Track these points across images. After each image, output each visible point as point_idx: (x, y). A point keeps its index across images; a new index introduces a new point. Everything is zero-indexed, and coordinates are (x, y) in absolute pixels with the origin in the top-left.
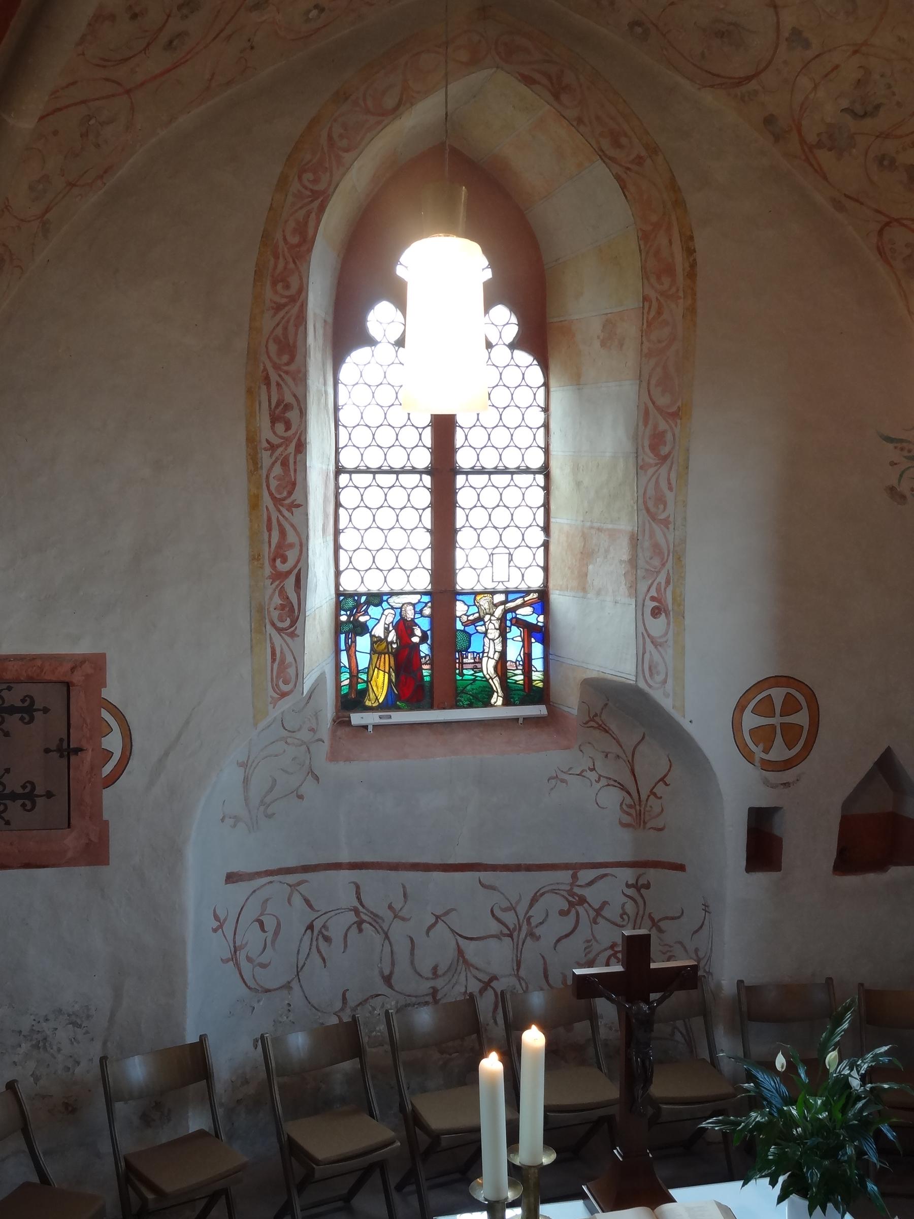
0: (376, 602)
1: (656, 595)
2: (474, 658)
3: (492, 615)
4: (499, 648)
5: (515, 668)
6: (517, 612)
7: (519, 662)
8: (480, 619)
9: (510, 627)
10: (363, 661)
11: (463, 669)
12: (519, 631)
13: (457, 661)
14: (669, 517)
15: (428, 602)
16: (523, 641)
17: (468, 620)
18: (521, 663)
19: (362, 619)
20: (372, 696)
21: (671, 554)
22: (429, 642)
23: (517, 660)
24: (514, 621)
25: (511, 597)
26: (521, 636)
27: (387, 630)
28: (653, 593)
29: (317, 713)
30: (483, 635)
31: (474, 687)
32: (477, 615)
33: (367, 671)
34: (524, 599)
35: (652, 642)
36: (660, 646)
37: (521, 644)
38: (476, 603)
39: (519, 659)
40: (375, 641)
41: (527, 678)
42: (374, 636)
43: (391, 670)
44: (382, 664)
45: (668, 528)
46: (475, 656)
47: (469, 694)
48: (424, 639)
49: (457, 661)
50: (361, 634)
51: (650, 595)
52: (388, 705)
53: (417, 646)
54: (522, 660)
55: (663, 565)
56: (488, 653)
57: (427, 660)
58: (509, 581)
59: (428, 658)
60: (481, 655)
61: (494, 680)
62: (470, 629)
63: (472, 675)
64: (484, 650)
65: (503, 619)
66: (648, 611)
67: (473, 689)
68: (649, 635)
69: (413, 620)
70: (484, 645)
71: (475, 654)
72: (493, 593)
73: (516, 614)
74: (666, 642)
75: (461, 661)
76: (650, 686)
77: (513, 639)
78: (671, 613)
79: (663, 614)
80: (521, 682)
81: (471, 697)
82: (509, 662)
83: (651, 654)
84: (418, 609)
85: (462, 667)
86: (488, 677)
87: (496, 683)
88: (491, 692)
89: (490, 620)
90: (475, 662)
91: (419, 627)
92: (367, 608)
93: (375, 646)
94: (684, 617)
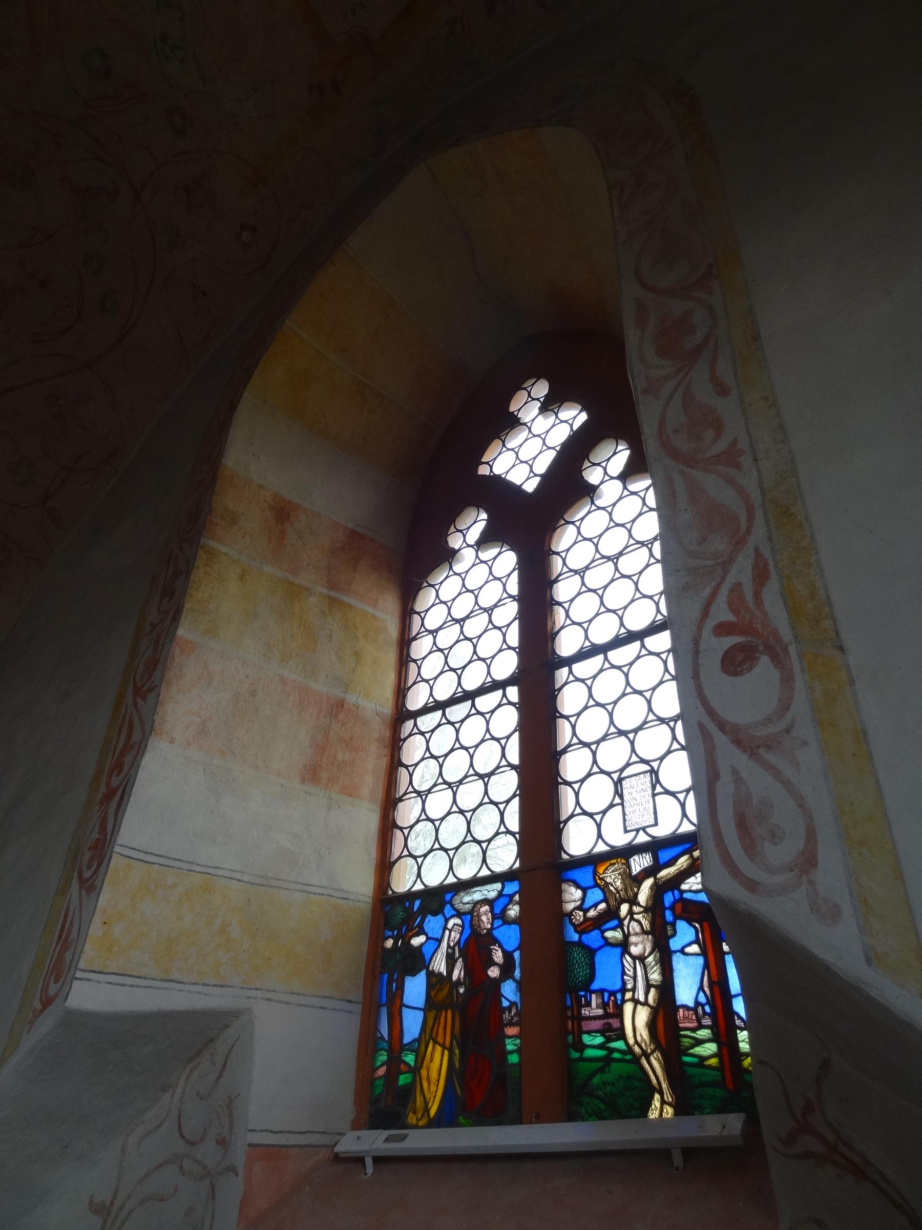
0: (435, 905)
1: (730, 617)
2: (604, 1005)
3: (633, 901)
4: (655, 976)
5: (695, 1025)
6: (684, 887)
7: (703, 1006)
8: (611, 914)
9: (673, 925)
10: (412, 1024)
11: (581, 1032)
12: (693, 930)
13: (569, 1014)
14: (735, 442)
15: (515, 894)
16: (704, 953)
17: (586, 919)
18: (707, 1009)
19: (417, 941)
20: (419, 1100)
21: (759, 514)
22: (517, 973)
23: (697, 1003)
24: (679, 907)
25: (664, 856)
26: (697, 941)
27: (451, 962)
28: (722, 613)
29: (231, 1101)
30: (618, 951)
31: (607, 1077)
32: (603, 906)
33: (418, 1048)
34: (692, 856)
35: (738, 742)
36: (769, 748)
37: (700, 960)
38: (599, 882)
39: (702, 999)
40: (435, 981)
41: (725, 1051)
42: (433, 971)
43: (455, 1043)
44: (441, 1031)
45: (738, 466)
46: (606, 1000)
47: (597, 1097)
48: (507, 970)
49: (569, 1014)
50: (413, 973)
51: (711, 623)
52: (445, 1119)
53: (497, 983)
54: (708, 1003)
55: (739, 542)
56: (634, 990)
57: (513, 1014)
58: (656, 824)
59: (514, 1011)
60: (619, 996)
61: (652, 1058)
62: (592, 939)
63: (600, 1047)
64: (624, 983)
65: (655, 907)
66: (712, 661)
67: (605, 1083)
68: (722, 726)
69: (490, 931)
70: (623, 973)
71: (606, 995)
72: (627, 852)
73: (682, 892)
74: (788, 731)
75: (575, 1013)
76: (752, 885)
77: (682, 951)
78: (792, 650)
79: (765, 661)
80: (713, 1061)
81: (602, 1106)
82: (681, 1010)
83: (738, 780)
84: (497, 910)
85: (580, 1027)
86: (637, 1049)
87: (655, 1066)
88: (648, 1091)
89: (631, 913)
90: (606, 1015)
91: (501, 946)
92: (423, 921)
93: (433, 993)
94: (841, 649)
